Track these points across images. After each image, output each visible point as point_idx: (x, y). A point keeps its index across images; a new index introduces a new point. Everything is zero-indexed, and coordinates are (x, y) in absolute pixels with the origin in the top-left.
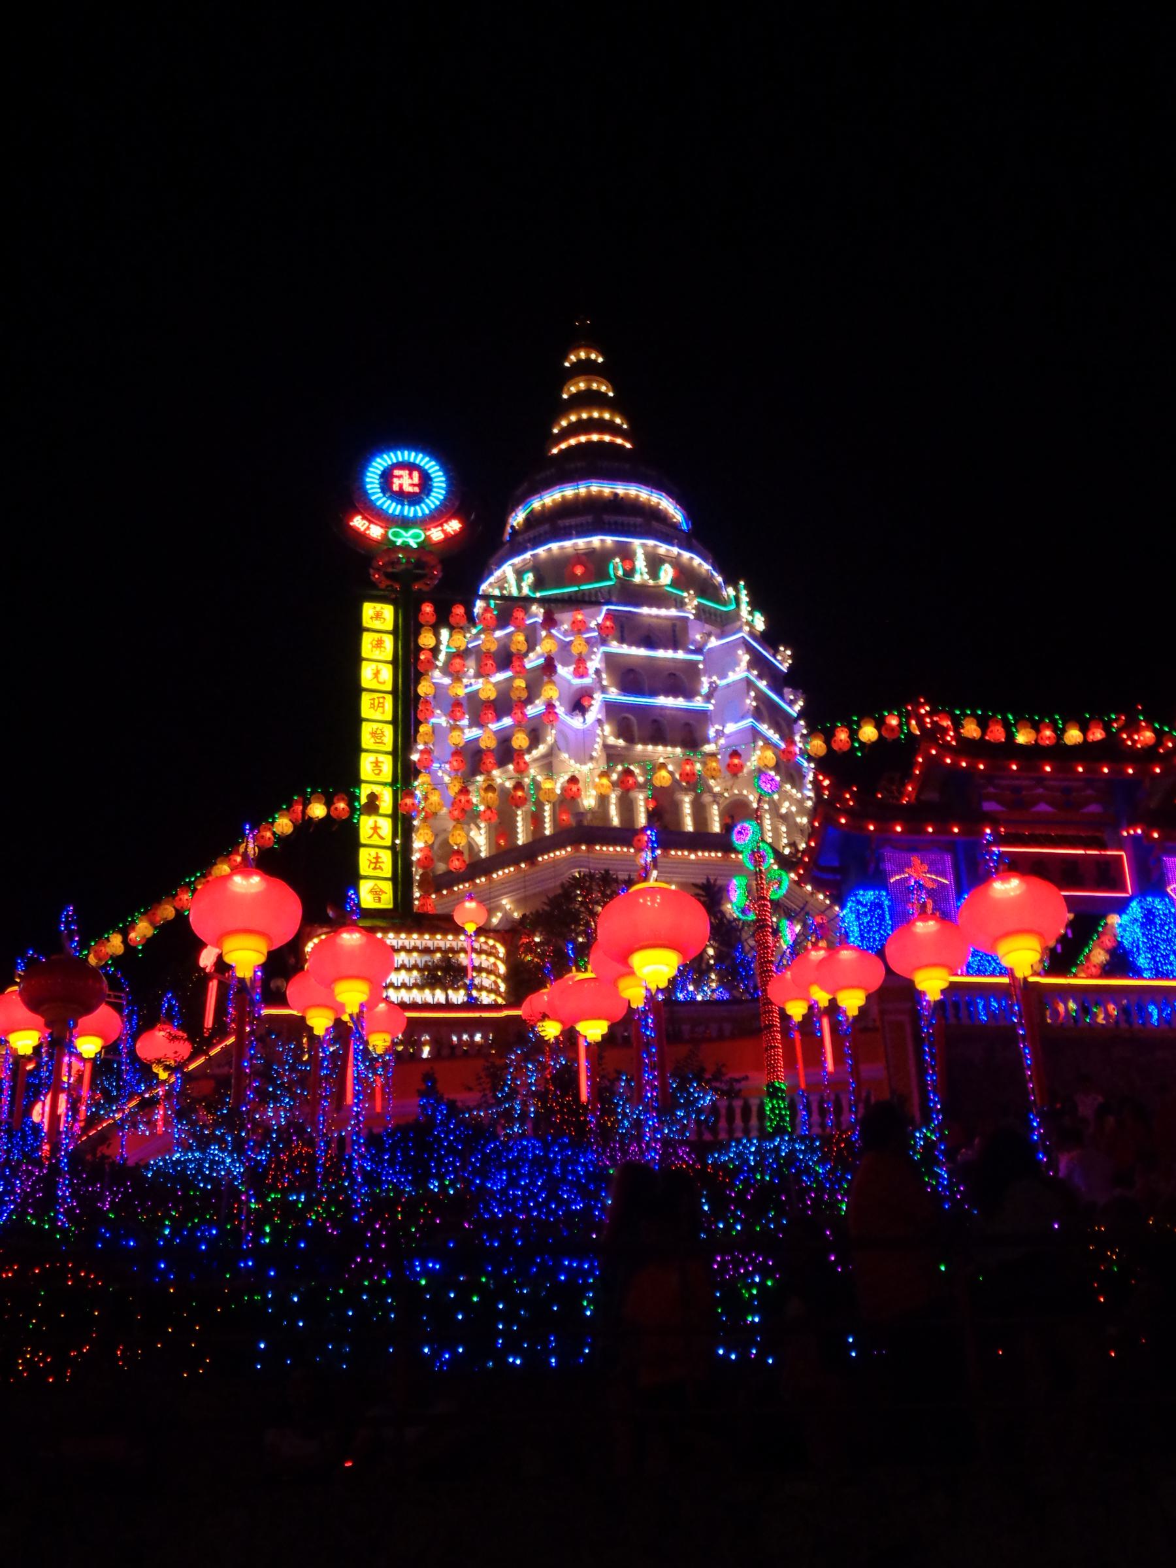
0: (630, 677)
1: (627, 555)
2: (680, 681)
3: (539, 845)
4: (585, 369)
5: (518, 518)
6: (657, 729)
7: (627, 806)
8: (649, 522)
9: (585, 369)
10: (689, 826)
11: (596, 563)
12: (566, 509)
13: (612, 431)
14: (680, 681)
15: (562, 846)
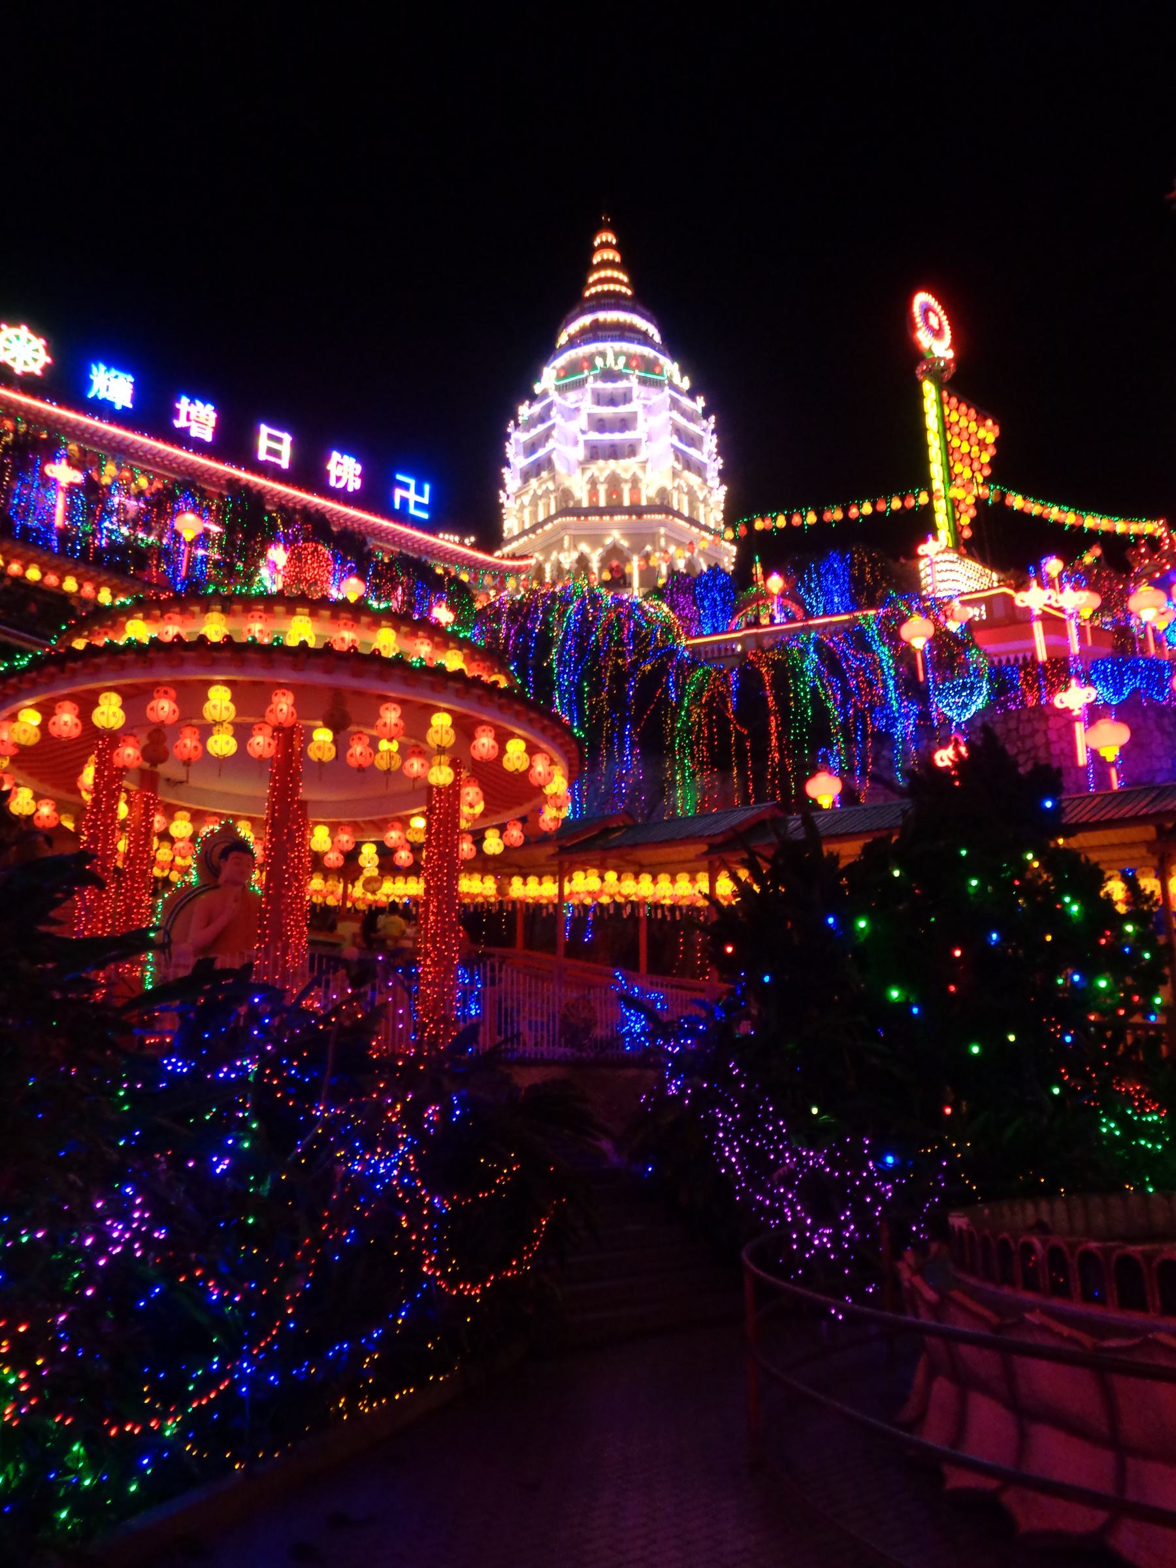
0: (600, 425)
1: (603, 355)
2: (625, 424)
3: (550, 519)
4: (605, 245)
5: (563, 339)
6: (614, 452)
7: (593, 492)
8: (623, 332)
9: (605, 245)
10: (626, 502)
11: (590, 360)
12: (583, 331)
13: (619, 282)
14: (625, 424)
15: (660, 513)
